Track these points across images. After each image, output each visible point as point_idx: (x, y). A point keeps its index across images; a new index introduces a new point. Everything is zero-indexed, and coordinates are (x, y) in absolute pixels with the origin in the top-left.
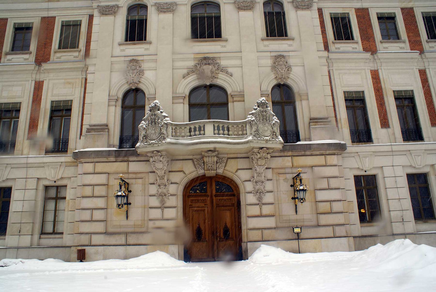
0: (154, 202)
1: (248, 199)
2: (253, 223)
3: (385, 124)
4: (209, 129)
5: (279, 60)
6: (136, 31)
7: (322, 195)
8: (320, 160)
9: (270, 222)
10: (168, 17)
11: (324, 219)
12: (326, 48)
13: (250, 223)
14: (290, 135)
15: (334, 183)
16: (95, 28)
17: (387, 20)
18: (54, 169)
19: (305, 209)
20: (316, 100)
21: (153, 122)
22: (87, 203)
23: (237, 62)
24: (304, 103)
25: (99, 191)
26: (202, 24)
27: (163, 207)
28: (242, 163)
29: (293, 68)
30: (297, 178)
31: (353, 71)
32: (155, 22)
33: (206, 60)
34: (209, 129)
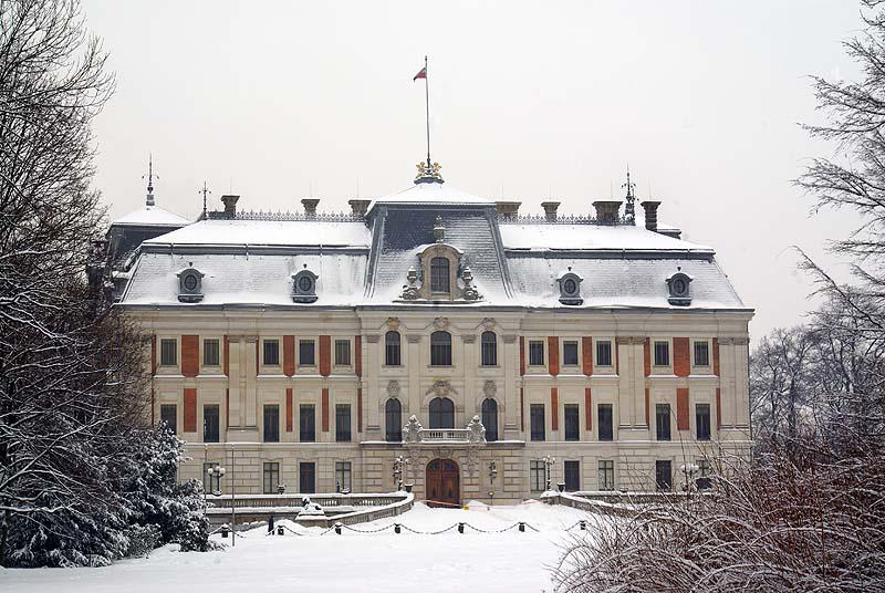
0: (411, 475)
1: (464, 474)
2: (467, 488)
3: (555, 427)
4: (445, 435)
5: (490, 385)
6: (393, 357)
7: (507, 474)
8: (508, 453)
9: (476, 488)
10: (413, 346)
11: (507, 488)
12: (523, 372)
13: (464, 489)
14: (491, 435)
15: (515, 467)
16: (364, 352)
17: (571, 347)
18: (345, 451)
19: (497, 482)
20: (509, 414)
21: (413, 428)
22: (370, 475)
23: (461, 383)
24: (503, 414)
25: (379, 468)
26: (438, 352)
27: (415, 478)
28: (461, 453)
29: (498, 390)
30: (492, 466)
31: (538, 385)
32: (406, 348)
33: (440, 383)
34: (445, 435)
